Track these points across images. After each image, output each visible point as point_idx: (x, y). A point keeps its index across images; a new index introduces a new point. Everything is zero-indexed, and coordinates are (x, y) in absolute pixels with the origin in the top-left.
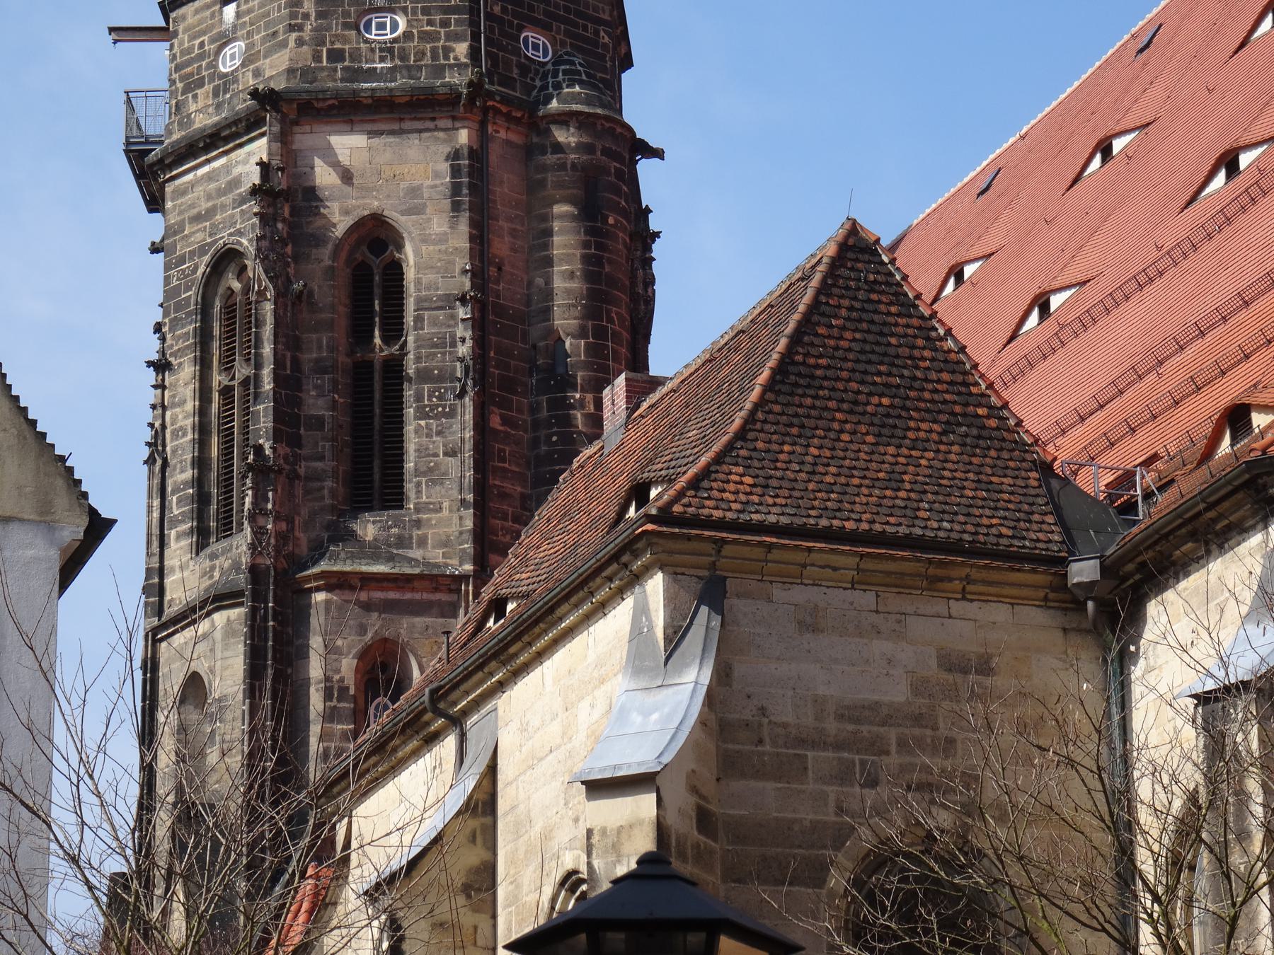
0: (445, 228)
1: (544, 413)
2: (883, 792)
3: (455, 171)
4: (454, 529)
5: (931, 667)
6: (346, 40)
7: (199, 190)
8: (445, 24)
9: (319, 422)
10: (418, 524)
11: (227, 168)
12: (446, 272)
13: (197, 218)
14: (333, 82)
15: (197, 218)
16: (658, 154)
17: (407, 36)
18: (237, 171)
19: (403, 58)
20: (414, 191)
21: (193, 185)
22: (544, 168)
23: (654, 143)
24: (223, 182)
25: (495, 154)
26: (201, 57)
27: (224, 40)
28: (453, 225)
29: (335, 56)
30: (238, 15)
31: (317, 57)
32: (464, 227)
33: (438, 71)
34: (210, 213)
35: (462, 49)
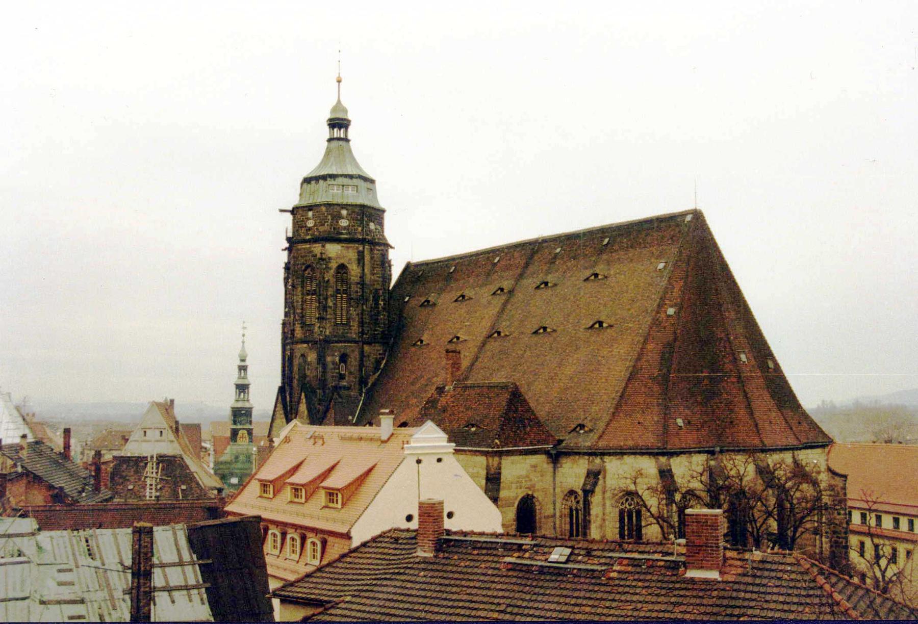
1: (373, 305)
2: (522, 490)
5: (529, 468)
17: (349, 226)
20: (350, 260)
23: (393, 246)
25: (365, 250)
28: (358, 266)
29: (334, 228)
31: (331, 228)
35: (360, 229)
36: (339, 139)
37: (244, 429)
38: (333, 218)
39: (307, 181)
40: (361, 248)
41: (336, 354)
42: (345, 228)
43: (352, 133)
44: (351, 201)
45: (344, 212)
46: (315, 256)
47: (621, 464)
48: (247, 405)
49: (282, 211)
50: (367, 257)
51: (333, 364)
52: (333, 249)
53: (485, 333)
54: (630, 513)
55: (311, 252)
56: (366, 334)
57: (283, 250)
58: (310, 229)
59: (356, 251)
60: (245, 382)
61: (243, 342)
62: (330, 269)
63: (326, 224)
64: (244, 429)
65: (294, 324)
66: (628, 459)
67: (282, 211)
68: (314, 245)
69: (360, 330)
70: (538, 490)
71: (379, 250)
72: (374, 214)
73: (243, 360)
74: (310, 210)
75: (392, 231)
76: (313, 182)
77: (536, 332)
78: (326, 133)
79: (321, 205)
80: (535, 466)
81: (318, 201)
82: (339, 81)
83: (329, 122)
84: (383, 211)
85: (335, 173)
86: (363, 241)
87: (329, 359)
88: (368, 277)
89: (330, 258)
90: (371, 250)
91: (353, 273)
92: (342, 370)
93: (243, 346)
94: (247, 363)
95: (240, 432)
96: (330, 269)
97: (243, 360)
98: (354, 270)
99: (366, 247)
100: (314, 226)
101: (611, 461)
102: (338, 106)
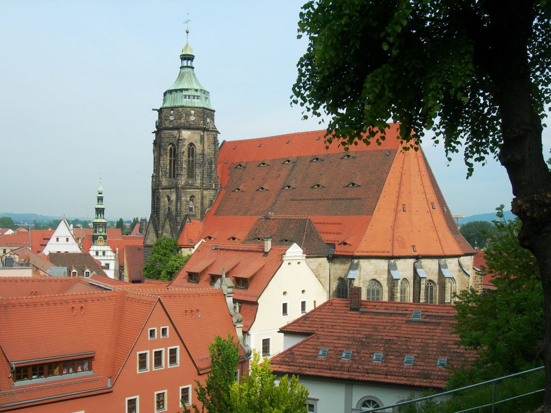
0: (200, 145)
3: (201, 138)
4: (200, 182)
6: (188, 120)
7: (167, 134)
8: (200, 119)
9: (185, 168)
10: (196, 181)
11: (172, 133)
12: (200, 150)
13: (167, 138)
14: (187, 125)
15: (167, 138)
16: (220, 133)
19: (195, 123)
20: (196, 140)
21: (166, 133)
22: (209, 137)
24: (171, 134)
26: (168, 116)
27: (171, 115)
29: (187, 122)
30: (173, 113)
33: (199, 125)
34: (169, 138)
35: (202, 122)
37: (101, 235)
38: (186, 115)
41: (188, 196)
42: (193, 121)
43: (195, 63)
44: (196, 106)
45: (193, 112)
46: (176, 137)
49: (153, 110)
50: (206, 139)
51: (186, 202)
52: (185, 134)
53: (281, 187)
54: (373, 291)
55: (173, 135)
56: (205, 184)
57: (153, 133)
58: (172, 121)
59: (200, 135)
62: (185, 145)
63: (182, 119)
64: (101, 235)
66: (373, 261)
67: (153, 110)
69: (202, 182)
70: (322, 277)
71: (211, 135)
74: (172, 110)
75: (219, 122)
76: (173, 93)
77: (312, 187)
79: (179, 107)
80: (320, 264)
82: (187, 32)
83: (182, 57)
85: (187, 88)
86: (204, 130)
87: (183, 199)
88: (207, 151)
89: (184, 139)
90: (208, 134)
91: (197, 148)
92: (191, 205)
95: (99, 237)
96: (185, 145)
98: (198, 148)
99: (205, 133)
100: (174, 119)
101: (364, 262)
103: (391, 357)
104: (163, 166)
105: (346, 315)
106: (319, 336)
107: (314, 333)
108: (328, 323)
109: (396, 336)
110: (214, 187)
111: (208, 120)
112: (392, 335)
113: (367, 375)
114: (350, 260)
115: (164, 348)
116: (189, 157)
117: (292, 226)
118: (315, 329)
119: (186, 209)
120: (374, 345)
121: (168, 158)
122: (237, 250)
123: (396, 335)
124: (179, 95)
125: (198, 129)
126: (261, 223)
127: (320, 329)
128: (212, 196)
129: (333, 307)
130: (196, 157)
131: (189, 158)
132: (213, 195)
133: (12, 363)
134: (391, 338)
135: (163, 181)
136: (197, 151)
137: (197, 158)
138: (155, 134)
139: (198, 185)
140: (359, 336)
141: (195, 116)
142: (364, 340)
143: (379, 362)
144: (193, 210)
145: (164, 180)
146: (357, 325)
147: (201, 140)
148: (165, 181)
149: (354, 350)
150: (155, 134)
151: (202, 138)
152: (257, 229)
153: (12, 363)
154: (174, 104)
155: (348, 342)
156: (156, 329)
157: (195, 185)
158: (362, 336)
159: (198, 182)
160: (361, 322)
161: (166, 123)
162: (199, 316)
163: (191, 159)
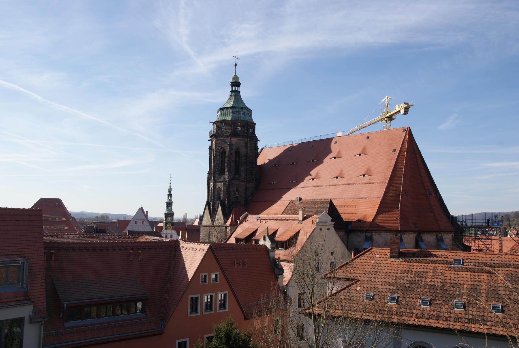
1: (251, 166)
3: (245, 143)
4: (244, 177)
6: (236, 130)
8: (245, 129)
13: (219, 143)
15: (219, 143)
16: (259, 141)
17: (241, 130)
18: (225, 140)
19: (241, 132)
20: (241, 145)
25: (248, 141)
29: (235, 131)
30: (225, 125)
32: (246, 149)
35: (246, 132)
36: (235, 91)
37: (170, 223)
39: (222, 109)
40: (246, 140)
41: (235, 187)
43: (241, 89)
45: (239, 124)
47: (380, 237)
48: (171, 212)
49: (210, 122)
50: (249, 145)
51: (234, 192)
52: (235, 140)
57: (209, 140)
58: (223, 131)
60: (170, 202)
61: (170, 183)
62: (233, 149)
64: (170, 223)
65: (215, 173)
68: (226, 138)
72: (253, 125)
73: (170, 192)
76: (225, 110)
78: (229, 88)
81: (228, 118)
82: (236, 65)
83: (231, 83)
84: (256, 124)
86: (247, 137)
87: (231, 189)
89: (233, 144)
90: (250, 141)
93: (170, 185)
94: (172, 193)
96: (233, 149)
97: (170, 192)
98: (243, 150)
99: (248, 140)
100: (225, 130)
101: (375, 235)
102: (236, 77)
103: (440, 302)
104: (216, 165)
105: (387, 262)
106: (362, 281)
107: (357, 279)
108: (369, 270)
109: (440, 282)
110: (255, 181)
111: (251, 130)
112: (436, 280)
113: (416, 320)
114: (364, 234)
115: (214, 293)
116: (236, 158)
117: (317, 207)
118: (357, 275)
119: (233, 197)
120: (419, 290)
121: (220, 159)
122: (276, 220)
123: (440, 280)
124: (229, 111)
125: (243, 136)
126: (292, 205)
127: (362, 275)
128: (253, 188)
129: (373, 255)
130: (241, 158)
131: (236, 159)
132: (254, 187)
133: (63, 303)
134: (436, 284)
135: (216, 176)
136: (242, 153)
137: (242, 158)
138: (210, 141)
139: (242, 179)
140: (402, 281)
141: (241, 127)
142: (408, 285)
143: (427, 306)
144: (239, 198)
145: (217, 176)
146: (399, 272)
147: (245, 145)
148: (217, 176)
149: (399, 295)
150: (210, 141)
151: (246, 143)
152: (289, 210)
153: (63, 303)
154: (225, 118)
155: (392, 287)
156: (207, 274)
157: (241, 179)
158: (405, 281)
159: (243, 177)
160: (402, 269)
161: (219, 132)
162: (246, 267)
163: (237, 160)
